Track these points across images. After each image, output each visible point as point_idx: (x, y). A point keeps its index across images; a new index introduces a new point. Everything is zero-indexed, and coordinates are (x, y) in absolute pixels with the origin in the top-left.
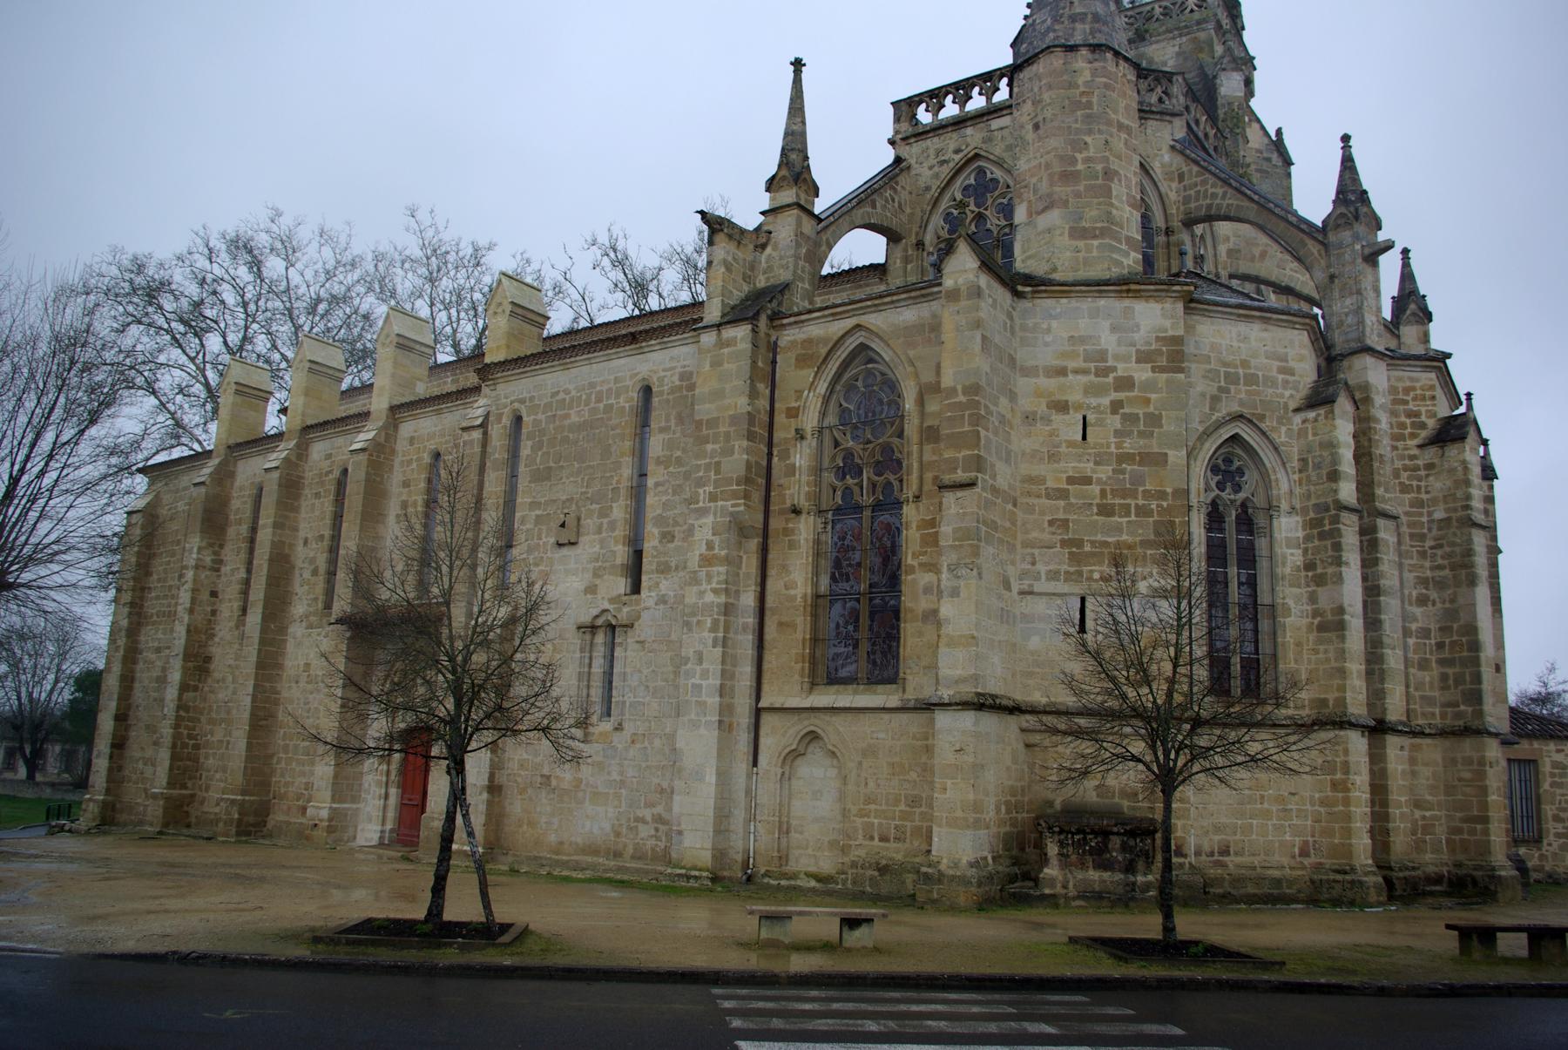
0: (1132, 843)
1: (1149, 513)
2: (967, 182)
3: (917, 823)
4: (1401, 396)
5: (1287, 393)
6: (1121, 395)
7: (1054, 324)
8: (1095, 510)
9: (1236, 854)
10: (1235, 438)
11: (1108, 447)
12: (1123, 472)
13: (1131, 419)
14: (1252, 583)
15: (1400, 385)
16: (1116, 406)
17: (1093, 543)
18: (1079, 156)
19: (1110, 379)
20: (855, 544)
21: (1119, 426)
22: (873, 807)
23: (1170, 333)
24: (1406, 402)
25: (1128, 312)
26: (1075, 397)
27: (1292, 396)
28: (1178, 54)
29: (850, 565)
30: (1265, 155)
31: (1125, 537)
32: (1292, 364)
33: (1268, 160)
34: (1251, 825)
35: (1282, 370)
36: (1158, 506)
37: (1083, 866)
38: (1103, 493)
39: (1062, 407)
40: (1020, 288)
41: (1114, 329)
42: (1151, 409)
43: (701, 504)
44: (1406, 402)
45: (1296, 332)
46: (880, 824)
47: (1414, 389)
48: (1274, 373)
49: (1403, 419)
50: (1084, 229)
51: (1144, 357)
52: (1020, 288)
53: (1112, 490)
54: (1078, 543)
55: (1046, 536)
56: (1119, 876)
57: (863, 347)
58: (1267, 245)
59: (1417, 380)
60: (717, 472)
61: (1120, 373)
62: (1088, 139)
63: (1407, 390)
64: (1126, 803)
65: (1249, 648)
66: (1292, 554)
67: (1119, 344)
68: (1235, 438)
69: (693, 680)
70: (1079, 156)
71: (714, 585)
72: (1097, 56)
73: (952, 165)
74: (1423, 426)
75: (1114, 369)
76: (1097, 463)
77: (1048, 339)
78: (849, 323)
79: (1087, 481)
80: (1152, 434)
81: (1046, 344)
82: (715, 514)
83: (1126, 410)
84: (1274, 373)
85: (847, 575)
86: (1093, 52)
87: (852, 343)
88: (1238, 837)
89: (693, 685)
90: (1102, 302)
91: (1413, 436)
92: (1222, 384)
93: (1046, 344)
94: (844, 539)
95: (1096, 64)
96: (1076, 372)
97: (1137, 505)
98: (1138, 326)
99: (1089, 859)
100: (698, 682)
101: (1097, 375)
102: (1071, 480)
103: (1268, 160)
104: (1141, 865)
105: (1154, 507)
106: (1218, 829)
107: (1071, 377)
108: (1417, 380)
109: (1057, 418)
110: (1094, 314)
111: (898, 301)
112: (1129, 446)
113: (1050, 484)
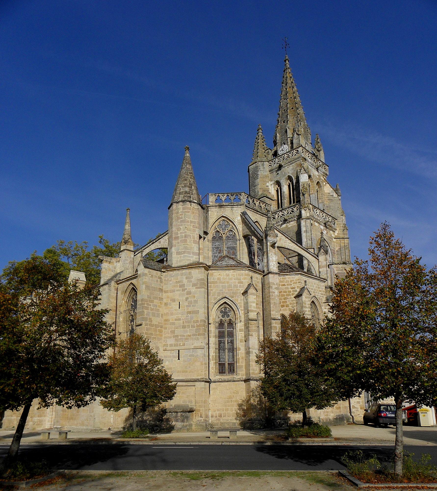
0: (183, 414)
4: (289, 283)
5: (241, 289)
7: (172, 278)
9: (224, 417)
10: (225, 303)
13: (191, 302)
14: (232, 342)
15: (289, 280)
16: (187, 299)
17: (181, 336)
18: (179, 232)
21: (187, 304)
23: (200, 278)
24: (291, 285)
25: (190, 273)
26: (177, 297)
27: (242, 289)
28: (292, 169)
30: (331, 194)
31: (188, 334)
32: (242, 280)
33: (333, 195)
34: (228, 408)
35: (239, 283)
39: (174, 300)
40: (163, 270)
41: (186, 278)
42: (195, 299)
44: (291, 285)
47: (293, 280)
48: (237, 284)
49: (290, 290)
51: (194, 285)
52: (163, 270)
54: (177, 336)
55: (170, 335)
58: (281, 236)
59: (294, 278)
62: (181, 227)
63: (291, 281)
64: (189, 404)
65: (231, 360)
66: (241, 333)
67: (188, 282)
68: (225, 303)
70: (179, 232)
72: (184, 204)
74: (296, 291)
75: (186, 289)
77: (171, 283)
79: (180, 319)
81: (170, 284)
83: (189, 300)
84: (237, 284)
86: (183, 203)
88: (224, 412)
90: (184, 271)
91: (293, 294)
92: (221, 289)
93: (170, 284)
95: (184, 206)
96: (177, 291)
98: (192, 277)
102: (176, 320)
103: (333, 195)
104: (186, 420)
105: (195, 325)
106: (218, 410)
108: (294, 278)
109: (173, 304)
110: (182, 274)
112: (190, 309)
113: (171, 321)
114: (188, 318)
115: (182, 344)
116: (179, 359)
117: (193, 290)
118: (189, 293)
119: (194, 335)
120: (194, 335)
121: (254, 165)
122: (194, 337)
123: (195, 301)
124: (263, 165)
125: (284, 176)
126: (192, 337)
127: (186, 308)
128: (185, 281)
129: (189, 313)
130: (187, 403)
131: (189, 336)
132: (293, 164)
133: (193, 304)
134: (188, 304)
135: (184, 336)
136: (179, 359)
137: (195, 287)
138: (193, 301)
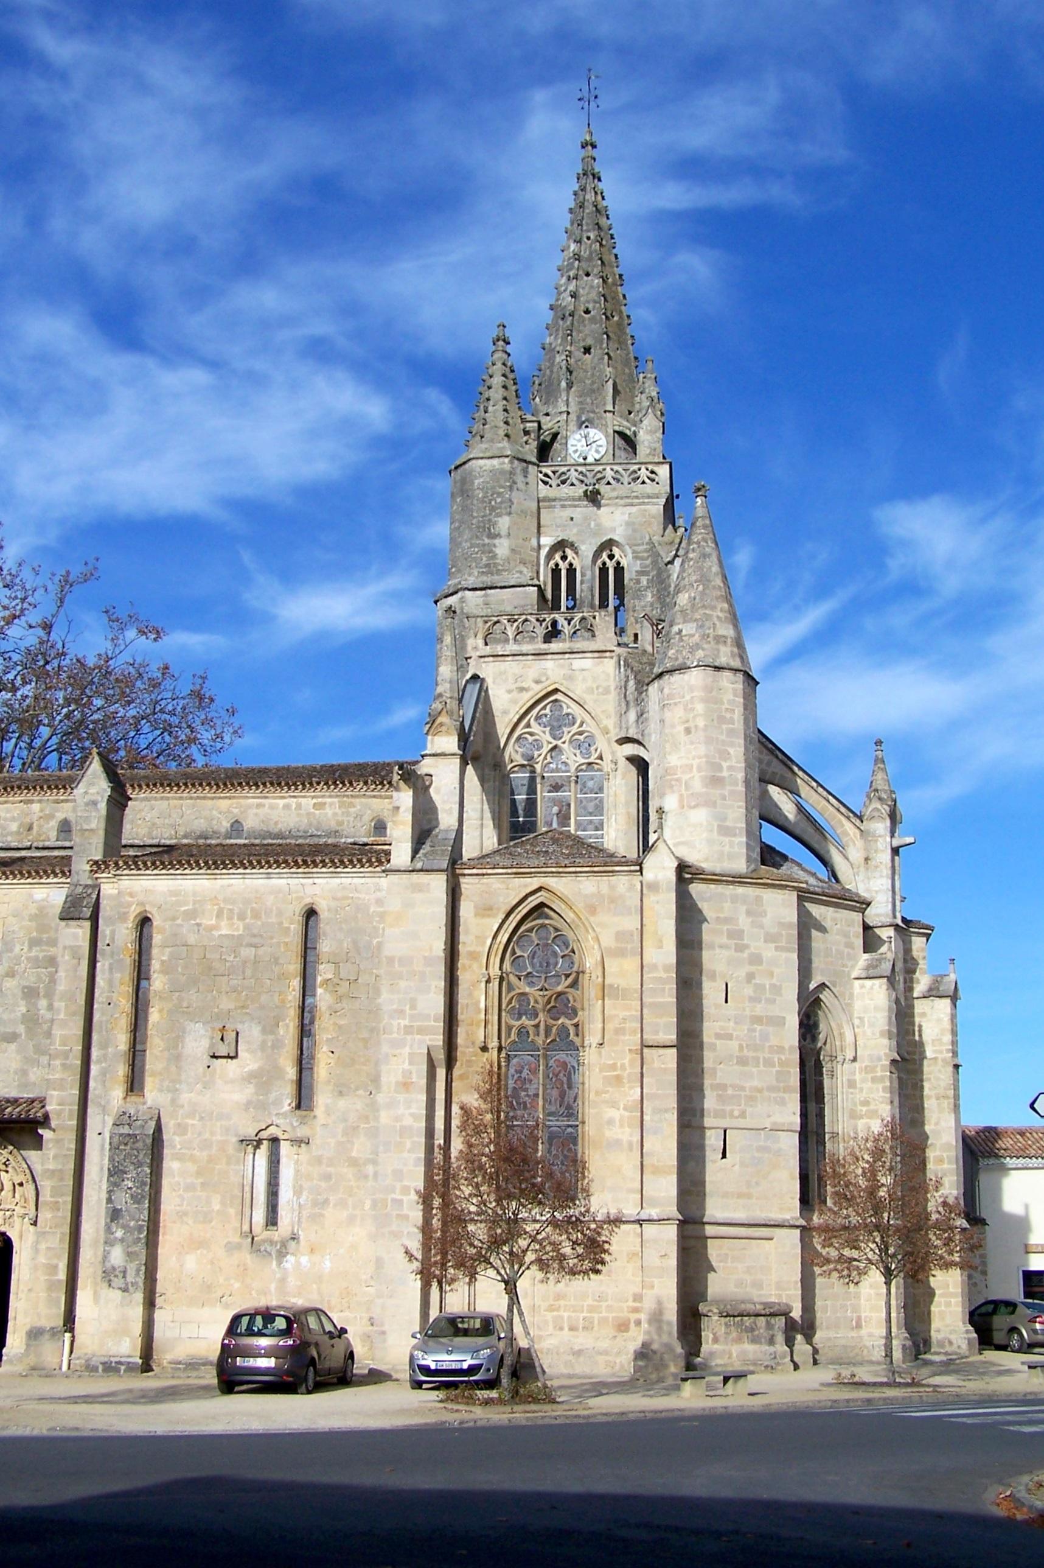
1: (772, 1065)
2: (543, 712)
3: (604, 1314)
6: (753, 968)
8: (735, 1061)
11: (744, 1010)
12: (754, 1030)
13: (760, 988)
16: (750, 977)
17: (733, 1086)
19: (746, 955)
20: (532, 1077)
21: (752, 994)
22: (562, 1303)
29: (528, 1095)
36: (779, 1059)
37: (739, 1340)
38: (741, 1047)
42: (774, 981)
43: (395, 1035)
45: (856, 913)
46: (569, 1317)
50: (728, 828)
51: (770, 938)
53: (747, 1045)
56: (766, 1348)
57: (542, 905)
60: (413, 1007)
61: (753, 950)
69: (393, 1196)
70: (725, 765)
71: (412, 1111)
73: (530, 694)
75: (747, 947)
76: (736, 1023)
78: (534, 883)
79: (729, 1037)
80: (775, 1000)
82: (411, 1046)
83: (757, 981)
85: (525, 1103)
87: (533, 902)
89: (394, 1200)
94: (521, 1072)
96: (721, 947)
97: (764, 1058)
98: (765, 912)
99: (745, 1335)
100: (399, 1197)
101: (736, 950)
105: (776, 1060)
107: (718, 951)
110: (734, 899)
111: (581, 872)
112: (759, 1009)
114: (754, 1034)
115: (736, 1113)
116: (724, 1156)
117: (768, 952)
118: (756, 959)
119: (771, 1089)
120: (771, 1089)
121: (495, 462)
122: (774, 1095)
123: (773, 986)
124: (525, 473)
125: (595, 534)
126: (766, 1094)
127: (747, 1004)
128: (744, 922)
129: (757, 1020)
130: (748, 1289)
131: (760, 1091)
132: (634, 509)
133: (768, 995)
134: (755, 992)
135: (743, 1088)
136: (724, 1156)
137: (773, 945)
138: (768, 986)
